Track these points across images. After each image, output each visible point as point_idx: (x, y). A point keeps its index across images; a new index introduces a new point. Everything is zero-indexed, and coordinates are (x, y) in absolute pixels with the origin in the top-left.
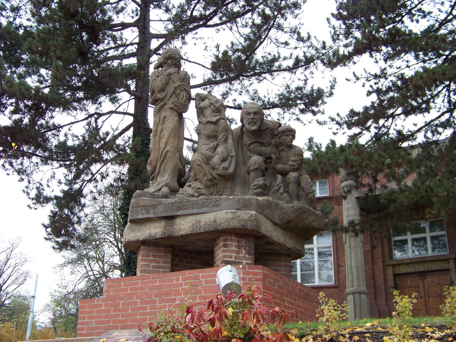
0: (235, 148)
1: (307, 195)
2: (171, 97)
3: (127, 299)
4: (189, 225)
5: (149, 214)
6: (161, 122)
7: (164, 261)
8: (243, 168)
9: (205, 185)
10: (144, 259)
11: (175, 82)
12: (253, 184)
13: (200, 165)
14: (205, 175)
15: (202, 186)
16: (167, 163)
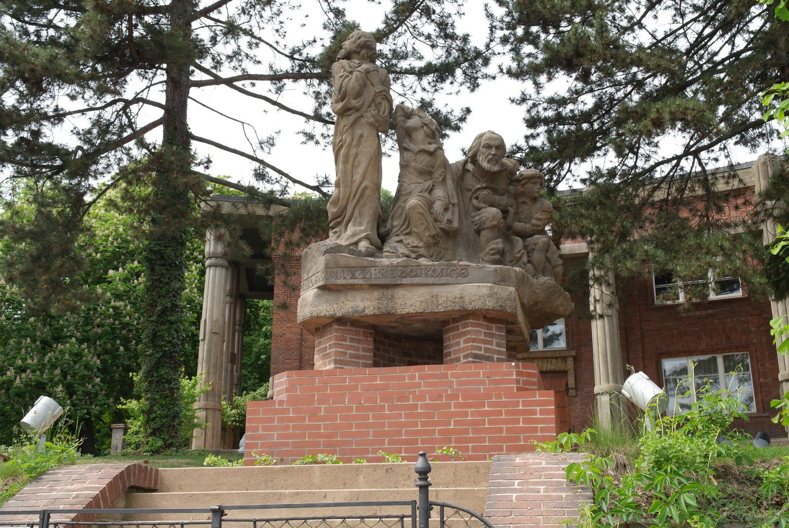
1: (553, 268)
2: (369, 106)
3: (333, 403)
4: (420, 299)
5: (355, 278)
6: (354, 143)
7: (365, 347)
9: (425, 243)
10: (339, 344)
11: (375, 84)
12: (490, 247)
13: (422, 214)
14: (427, 228)
15: (421, 244)
16: (365, 205)
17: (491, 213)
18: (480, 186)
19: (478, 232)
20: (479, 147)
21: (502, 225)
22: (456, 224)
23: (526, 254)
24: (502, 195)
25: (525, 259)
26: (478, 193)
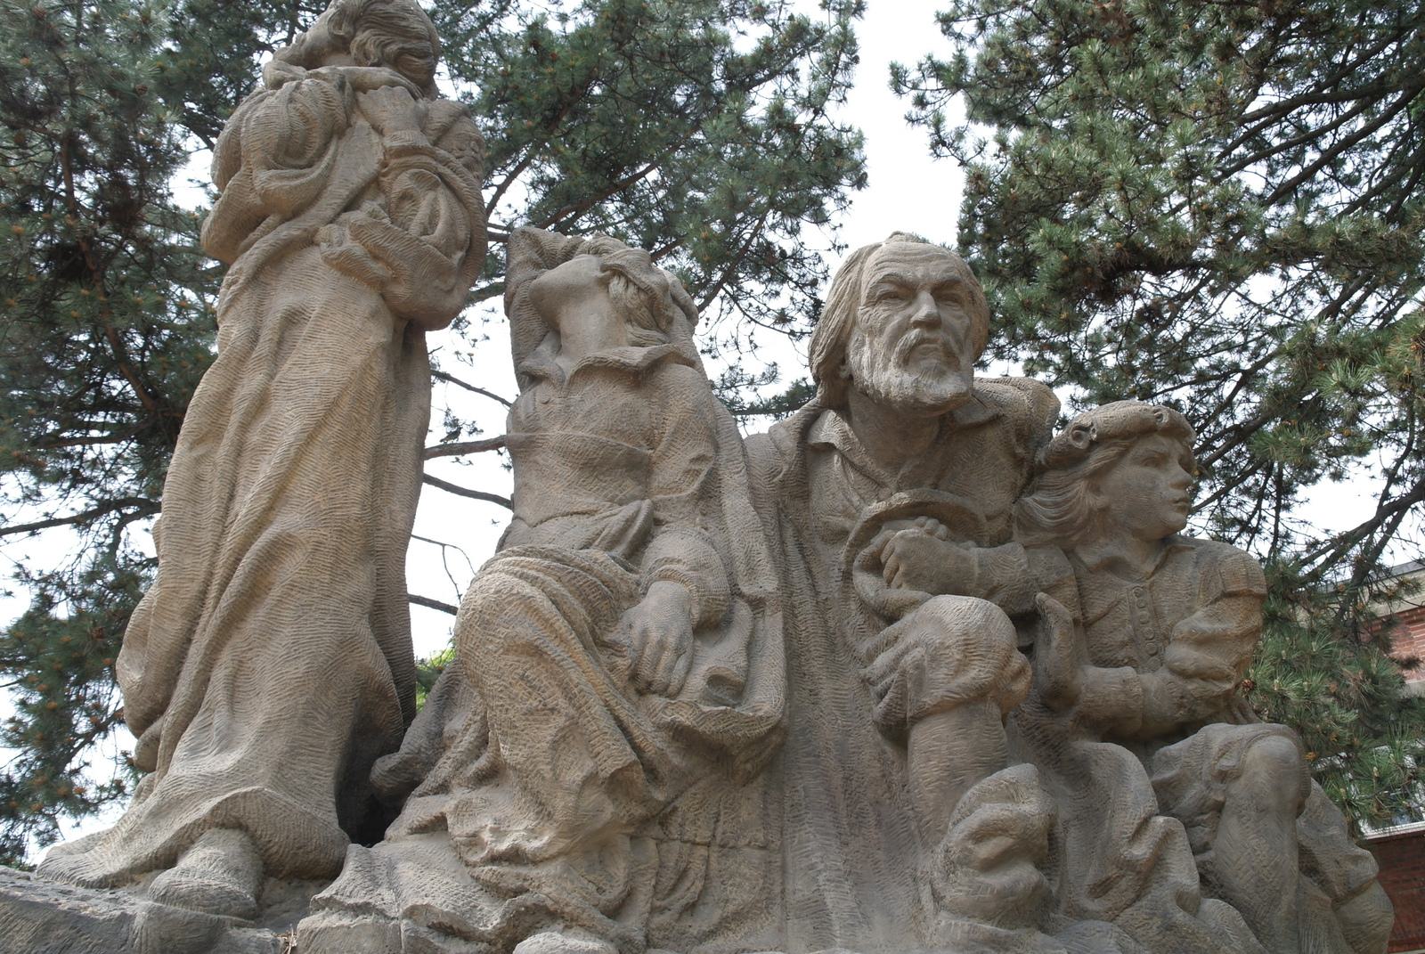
0: (771, 548)
1: (1338, 902)
2: (351, 204)
6: (264, 347)
8: (826, 689)
9: (570, 829)
11: (387, 125)
12: (973, 822)
13: (535, 651)
16: (268, 632)
17: (952, 623)
18: (876, 507)
19: (897, 732)
20: (851, 310)
21: (1020, 686)
22: (766, 699)
23: (1181, 841)
24: (1000, 540)
25: (1182, 872)
26: (877, 541)
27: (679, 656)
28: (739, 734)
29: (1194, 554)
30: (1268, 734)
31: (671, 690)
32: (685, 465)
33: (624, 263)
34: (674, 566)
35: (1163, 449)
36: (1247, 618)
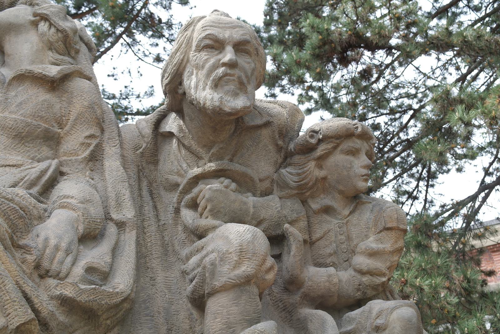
0: (132, 192)
8: (160, 277)
17: (235, 239)
18: (196, 171)
19: (199, 302)
20: (186, 53)
21: (270, 276)
22: (122, 281)
24: (266, 193)
26: (196, 190)
27: (68, 255)
28: (103, 302)
29: (370, 206)
30: (402, 306)
31: (61, 275)
32: (81, 140)
33: (48, 13)
34: (69, 200)
35: (357, 146)
36: (396, 242)
